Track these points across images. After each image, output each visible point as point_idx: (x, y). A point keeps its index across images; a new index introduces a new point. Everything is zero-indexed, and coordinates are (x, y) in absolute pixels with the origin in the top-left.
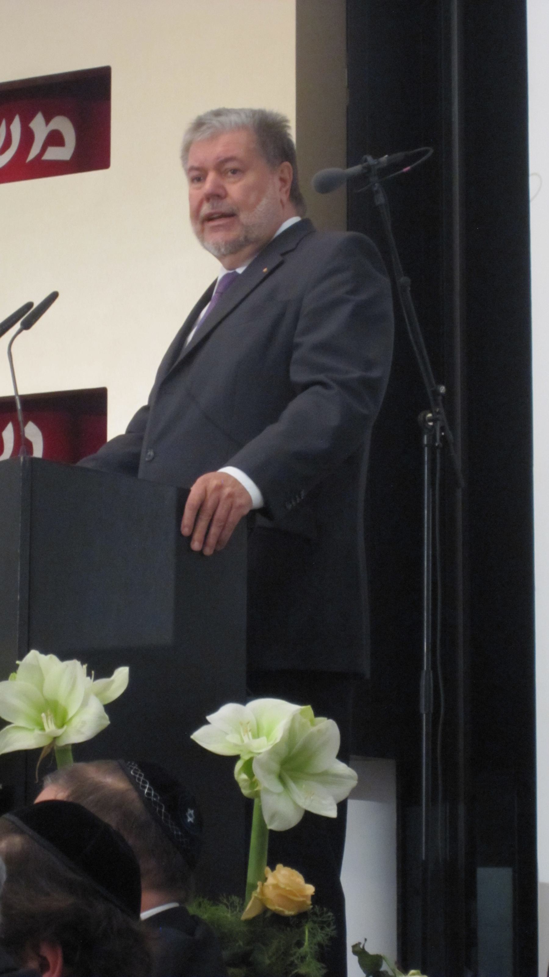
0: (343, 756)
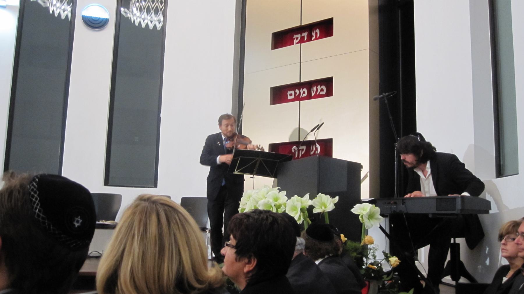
0: (381, 215)
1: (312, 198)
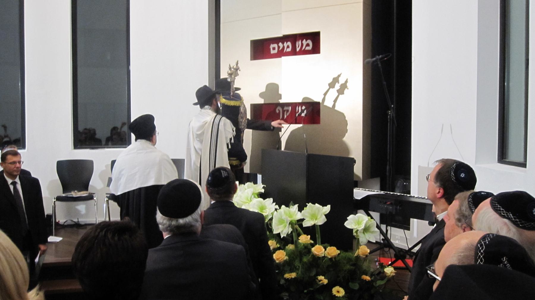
1: (300, 209)
